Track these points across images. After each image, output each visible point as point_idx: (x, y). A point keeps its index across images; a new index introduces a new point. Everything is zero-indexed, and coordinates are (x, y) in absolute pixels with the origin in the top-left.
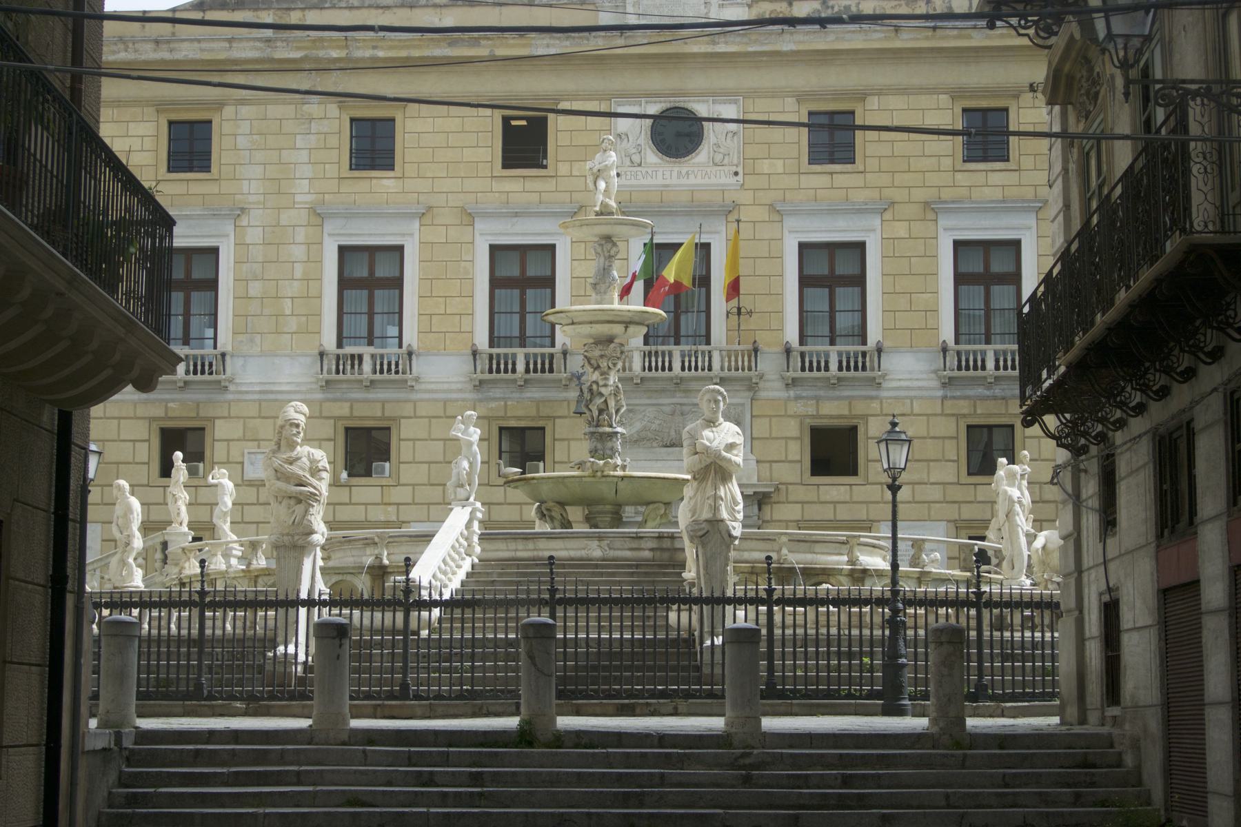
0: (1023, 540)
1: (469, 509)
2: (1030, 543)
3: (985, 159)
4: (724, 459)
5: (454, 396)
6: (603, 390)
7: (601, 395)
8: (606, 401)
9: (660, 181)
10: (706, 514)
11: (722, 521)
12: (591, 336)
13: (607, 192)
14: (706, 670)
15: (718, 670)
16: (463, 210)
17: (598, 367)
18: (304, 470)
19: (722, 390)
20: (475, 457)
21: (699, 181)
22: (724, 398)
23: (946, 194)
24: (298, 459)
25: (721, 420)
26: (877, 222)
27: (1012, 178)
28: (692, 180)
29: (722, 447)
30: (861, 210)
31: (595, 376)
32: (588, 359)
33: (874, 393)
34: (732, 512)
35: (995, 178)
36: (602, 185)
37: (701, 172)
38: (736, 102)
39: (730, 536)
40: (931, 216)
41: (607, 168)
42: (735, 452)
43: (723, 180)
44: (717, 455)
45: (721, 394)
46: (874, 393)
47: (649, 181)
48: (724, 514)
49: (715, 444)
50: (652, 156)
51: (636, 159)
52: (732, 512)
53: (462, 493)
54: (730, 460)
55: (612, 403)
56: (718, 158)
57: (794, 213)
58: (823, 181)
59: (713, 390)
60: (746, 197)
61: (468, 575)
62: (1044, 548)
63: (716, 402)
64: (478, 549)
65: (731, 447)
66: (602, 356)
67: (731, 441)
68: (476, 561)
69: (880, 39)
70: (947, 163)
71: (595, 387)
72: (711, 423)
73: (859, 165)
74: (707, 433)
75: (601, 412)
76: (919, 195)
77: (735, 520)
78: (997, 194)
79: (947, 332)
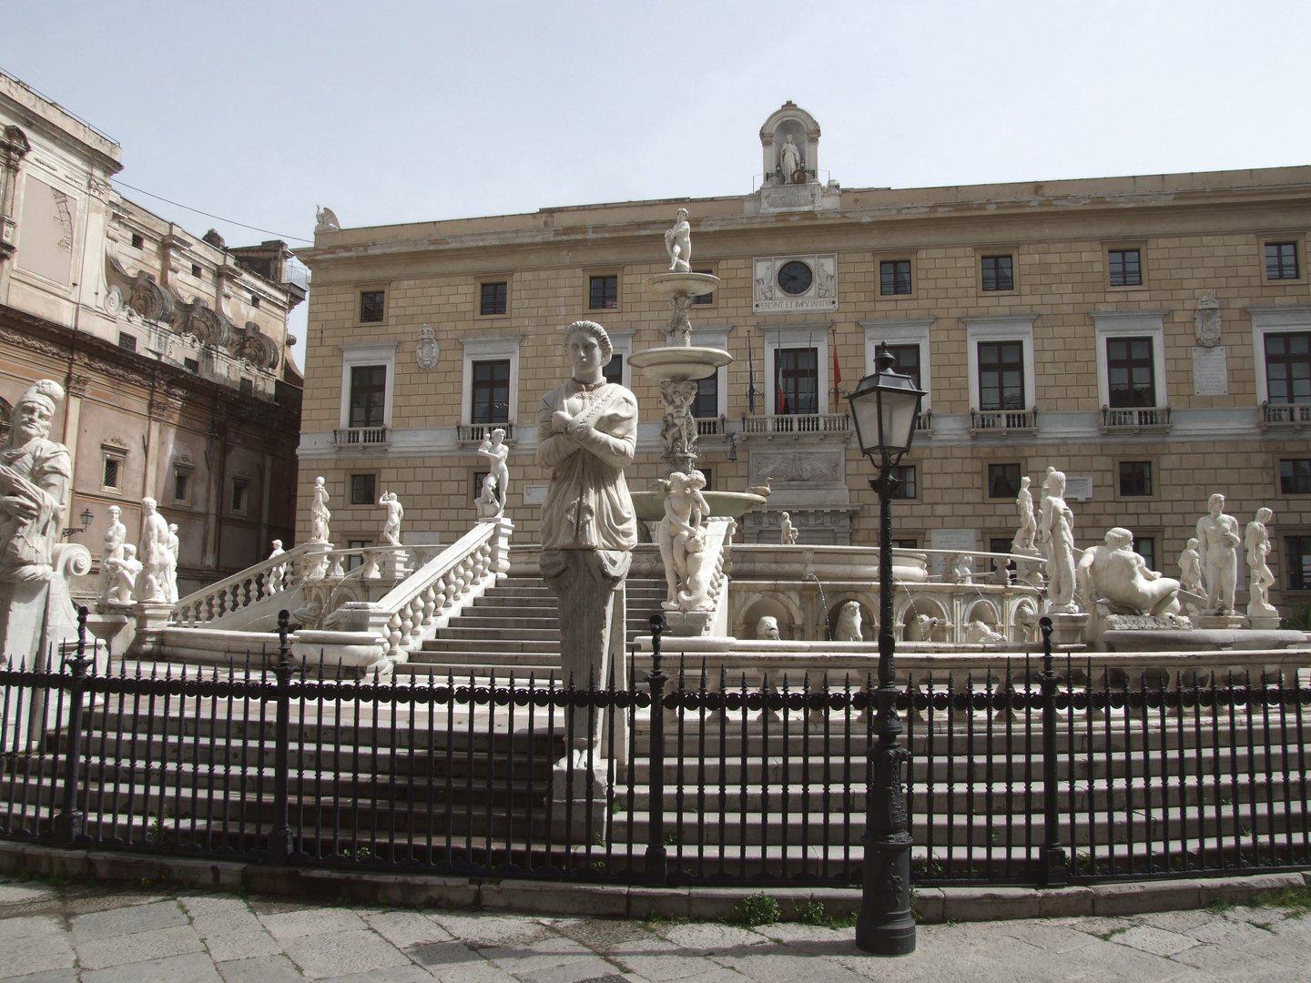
0: (1070, 558)
1: (493, 525)
2: (1077, 562)
3: (997, 289)
4: (596, 441)
5: (654, 450)
6: (677, 421)
7: (675, 425)
8: (679, 431)
9: (784, 309)
10: (564, 540)
11: (592, 549)
12: (666, 375)
13: (681, 256)
14: (559, 815)
15: (579, 816)
16: (659, 331)
17: (673, 401)
18: (21, 472)
19: (597, 326)
20: (502, 472)
21: (810, 308)
22: (603, 342)
23: (972, 312)
24: (21, 456)
25: (602, 379)
26: (926, 332)
27: (1015, 300)
28: (805, 308)
29: (592, 422)
30: (916, 323)
31: (670, 409)
32: (665, 396)
33: (926, 444)
34: (611, 535)
35: (1004, 301)
36: (677, 249)
37: (812, 302)
38: (833, 257)
39: (606, 576)
40: (961, 326)
41: (683, 234)
42: (619, 431)
43: (825, 307)
44: (584, 434)
45: (596, 334)
46: (926, 444)
47: (777, 309)
48: (594, 537)
49: (580, 417)
50: (779, 294)
51: (769, 295)
52: (611, 535)
53: (489, 510)
54: (606, 445)
55: (684, 433)
56: (822, 292)
57: (871, 327)
58: (891, 306)
59: (583, 328)
60: (840, 317)
61: (487, 592)
62: (1092, 566)
63: (588, 348)
64: (505, 564)
65: (609, 423)
66: (675, 392)
67: (609, 412)
68: (503, 576)
69: (926, 212)
70: (972, 291)
71: (669, 418)
72: (583, 383)
73: (914, 295)
74: (575, 401)
75: (675, 440)
76: (955, 313)
77: (620, 548)
78: (1006, 311)
79: (974, 403)
